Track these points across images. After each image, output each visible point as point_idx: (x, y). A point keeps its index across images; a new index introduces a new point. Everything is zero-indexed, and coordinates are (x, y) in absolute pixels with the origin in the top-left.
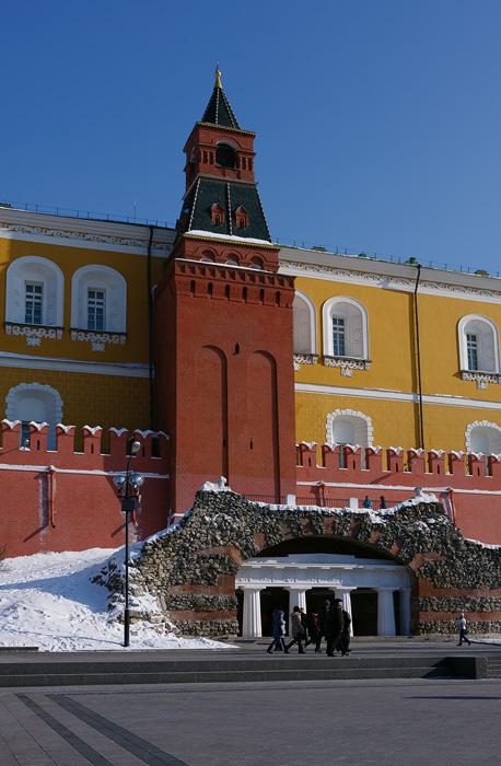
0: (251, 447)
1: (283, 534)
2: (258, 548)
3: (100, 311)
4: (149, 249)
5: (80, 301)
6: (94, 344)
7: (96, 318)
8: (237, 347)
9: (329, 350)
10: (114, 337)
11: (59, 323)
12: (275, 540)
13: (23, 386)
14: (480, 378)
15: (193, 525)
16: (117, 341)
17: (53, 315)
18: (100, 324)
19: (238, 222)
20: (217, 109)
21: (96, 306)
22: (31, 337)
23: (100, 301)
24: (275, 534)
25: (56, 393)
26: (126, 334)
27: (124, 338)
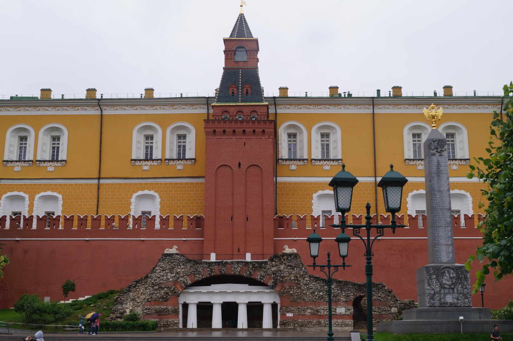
0: (247, 220)
1: (205, 273)
2: (189, 282)
4: (208, 109)
5: (171, 143)
7: (181, 149)
8: (240, 164)
9: (317, 154)
11: (160, 157)
12: (199, 277)
13: (140, 193)
14: (418, 162)
15: (158, 271)
17: (157, 154)
18: (184, 154)
19: (245, 92)
20: (241, 21)
21: (182, 144)
22: (145, 165)
23: (184, 141)
24: (199, 274)
25: (156, 194)
26: (195, 159)
27: (194, 161)
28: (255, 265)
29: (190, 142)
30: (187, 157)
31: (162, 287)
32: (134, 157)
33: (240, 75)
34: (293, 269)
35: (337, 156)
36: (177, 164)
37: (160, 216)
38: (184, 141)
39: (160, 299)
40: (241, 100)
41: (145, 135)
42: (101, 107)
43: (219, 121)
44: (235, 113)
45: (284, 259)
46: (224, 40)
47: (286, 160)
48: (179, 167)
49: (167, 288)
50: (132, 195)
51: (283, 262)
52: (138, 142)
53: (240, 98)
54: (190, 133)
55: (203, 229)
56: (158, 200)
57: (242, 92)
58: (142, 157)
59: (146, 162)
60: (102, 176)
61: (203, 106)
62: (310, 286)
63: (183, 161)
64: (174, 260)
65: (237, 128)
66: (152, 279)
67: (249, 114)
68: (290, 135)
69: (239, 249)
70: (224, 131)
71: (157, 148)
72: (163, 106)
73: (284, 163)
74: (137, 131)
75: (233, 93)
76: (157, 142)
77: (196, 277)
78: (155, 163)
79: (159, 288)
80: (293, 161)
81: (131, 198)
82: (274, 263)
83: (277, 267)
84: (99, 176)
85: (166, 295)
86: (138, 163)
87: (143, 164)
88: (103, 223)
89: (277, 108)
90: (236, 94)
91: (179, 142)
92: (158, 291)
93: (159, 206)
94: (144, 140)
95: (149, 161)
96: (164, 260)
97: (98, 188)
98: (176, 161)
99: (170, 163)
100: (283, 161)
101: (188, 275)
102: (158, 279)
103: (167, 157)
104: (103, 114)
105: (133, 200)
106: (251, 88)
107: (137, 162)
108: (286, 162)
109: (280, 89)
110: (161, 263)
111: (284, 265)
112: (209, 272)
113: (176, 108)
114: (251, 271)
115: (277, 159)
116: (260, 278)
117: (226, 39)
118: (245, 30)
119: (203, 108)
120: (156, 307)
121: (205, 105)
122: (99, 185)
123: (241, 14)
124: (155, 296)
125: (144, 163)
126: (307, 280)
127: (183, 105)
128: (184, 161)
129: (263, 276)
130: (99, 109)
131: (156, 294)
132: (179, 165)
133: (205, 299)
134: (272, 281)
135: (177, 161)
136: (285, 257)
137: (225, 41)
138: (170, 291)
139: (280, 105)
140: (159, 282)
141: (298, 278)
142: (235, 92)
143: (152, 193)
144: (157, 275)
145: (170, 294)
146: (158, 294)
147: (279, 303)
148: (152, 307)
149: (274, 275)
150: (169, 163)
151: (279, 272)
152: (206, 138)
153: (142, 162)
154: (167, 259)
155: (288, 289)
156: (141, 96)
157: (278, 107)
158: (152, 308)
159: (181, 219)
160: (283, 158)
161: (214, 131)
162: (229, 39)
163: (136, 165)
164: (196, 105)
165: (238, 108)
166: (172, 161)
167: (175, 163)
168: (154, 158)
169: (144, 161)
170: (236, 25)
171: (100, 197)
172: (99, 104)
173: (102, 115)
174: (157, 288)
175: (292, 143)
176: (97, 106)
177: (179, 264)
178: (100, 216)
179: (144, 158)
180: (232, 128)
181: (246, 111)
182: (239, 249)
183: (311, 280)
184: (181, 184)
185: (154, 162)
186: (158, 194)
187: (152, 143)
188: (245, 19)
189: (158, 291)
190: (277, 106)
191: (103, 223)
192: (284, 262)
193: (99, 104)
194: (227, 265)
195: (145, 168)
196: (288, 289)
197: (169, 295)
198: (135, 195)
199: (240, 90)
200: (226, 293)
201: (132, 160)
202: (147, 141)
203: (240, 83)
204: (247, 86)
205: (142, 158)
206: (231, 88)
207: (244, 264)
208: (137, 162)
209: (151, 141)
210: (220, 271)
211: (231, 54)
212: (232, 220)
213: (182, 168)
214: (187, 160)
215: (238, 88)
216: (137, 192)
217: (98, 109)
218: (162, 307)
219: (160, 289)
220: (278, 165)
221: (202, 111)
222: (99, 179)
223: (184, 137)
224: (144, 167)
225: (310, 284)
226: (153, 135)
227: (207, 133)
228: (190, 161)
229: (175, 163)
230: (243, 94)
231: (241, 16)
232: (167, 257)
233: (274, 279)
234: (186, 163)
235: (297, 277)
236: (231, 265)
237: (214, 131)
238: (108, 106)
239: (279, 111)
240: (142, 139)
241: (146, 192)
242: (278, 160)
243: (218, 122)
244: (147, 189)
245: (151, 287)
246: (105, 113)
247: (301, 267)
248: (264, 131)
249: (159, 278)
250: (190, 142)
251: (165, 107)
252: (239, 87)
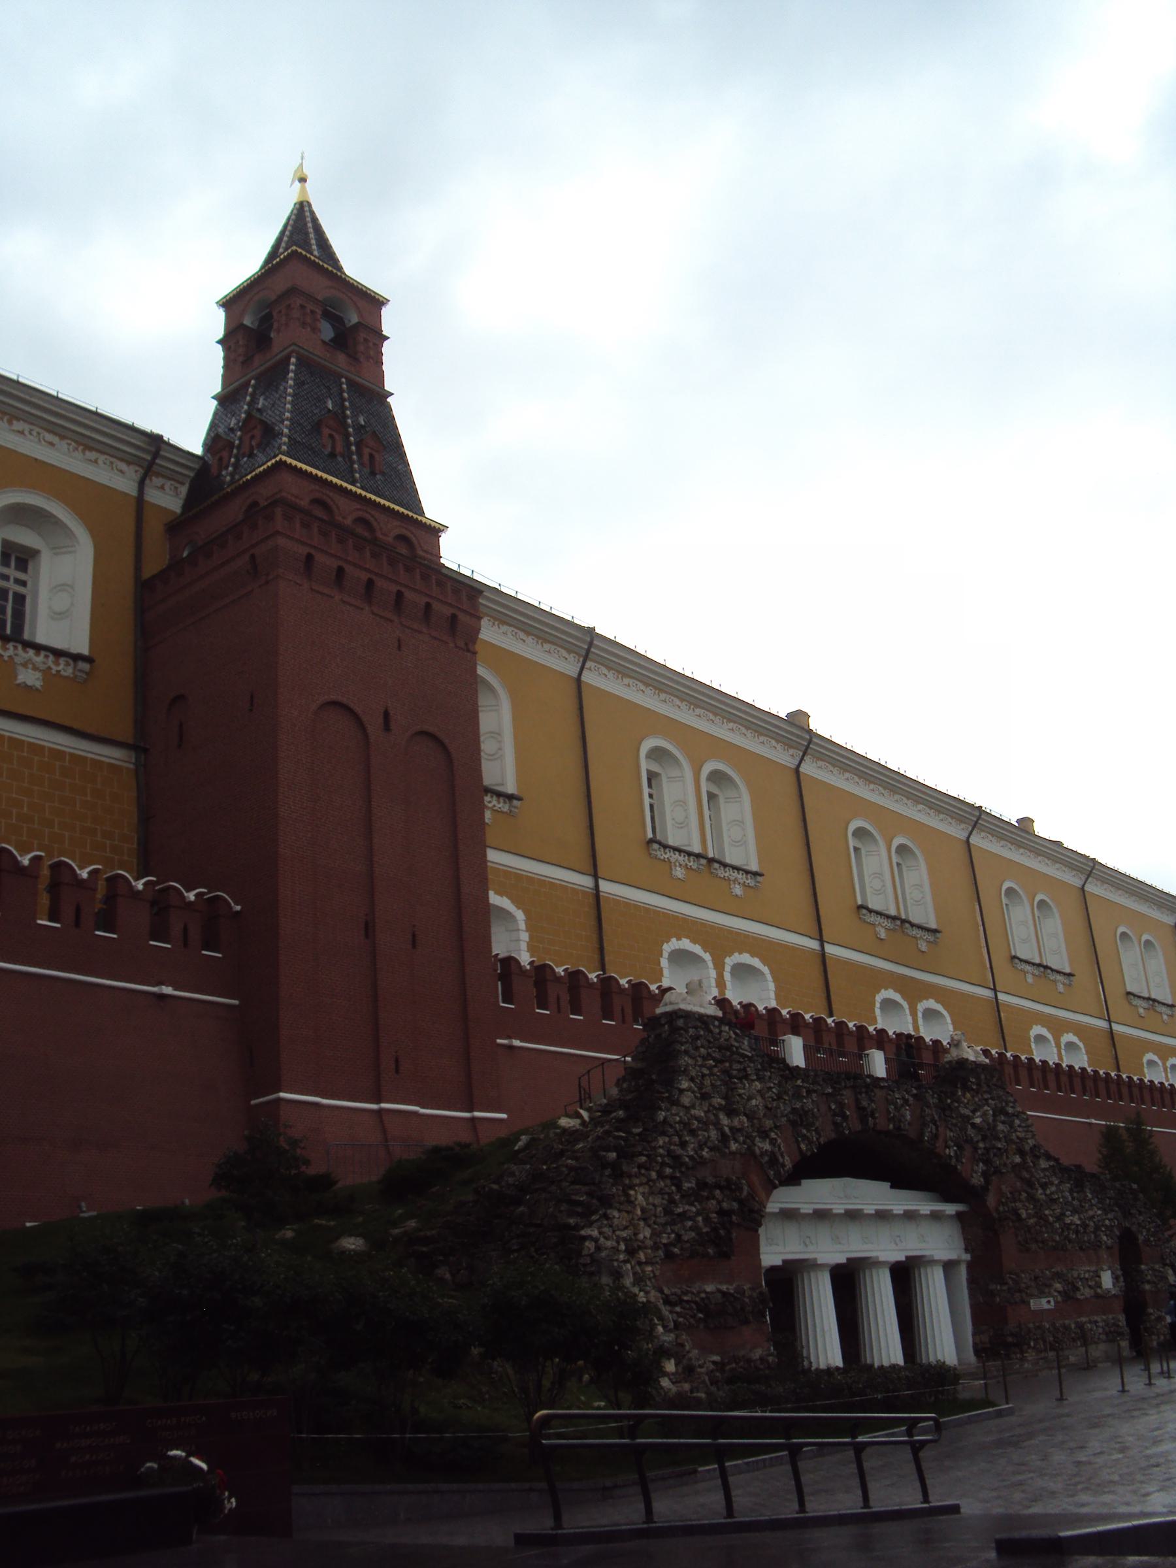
6: (20, 669)
10: (62, 661)
16: (69, 672)
19: (366, 458)
27: (85, 666)
35: (502, 785)
36: (17, 660)
113: (22, 433)
127: (49, 431)
132: (25, 665)
184: (35, 749)
212: (367, 936)
213: (38, 684)
221: (123, 481)
229: (11, 652)
234: (55, 668)
245: (668, 1182)
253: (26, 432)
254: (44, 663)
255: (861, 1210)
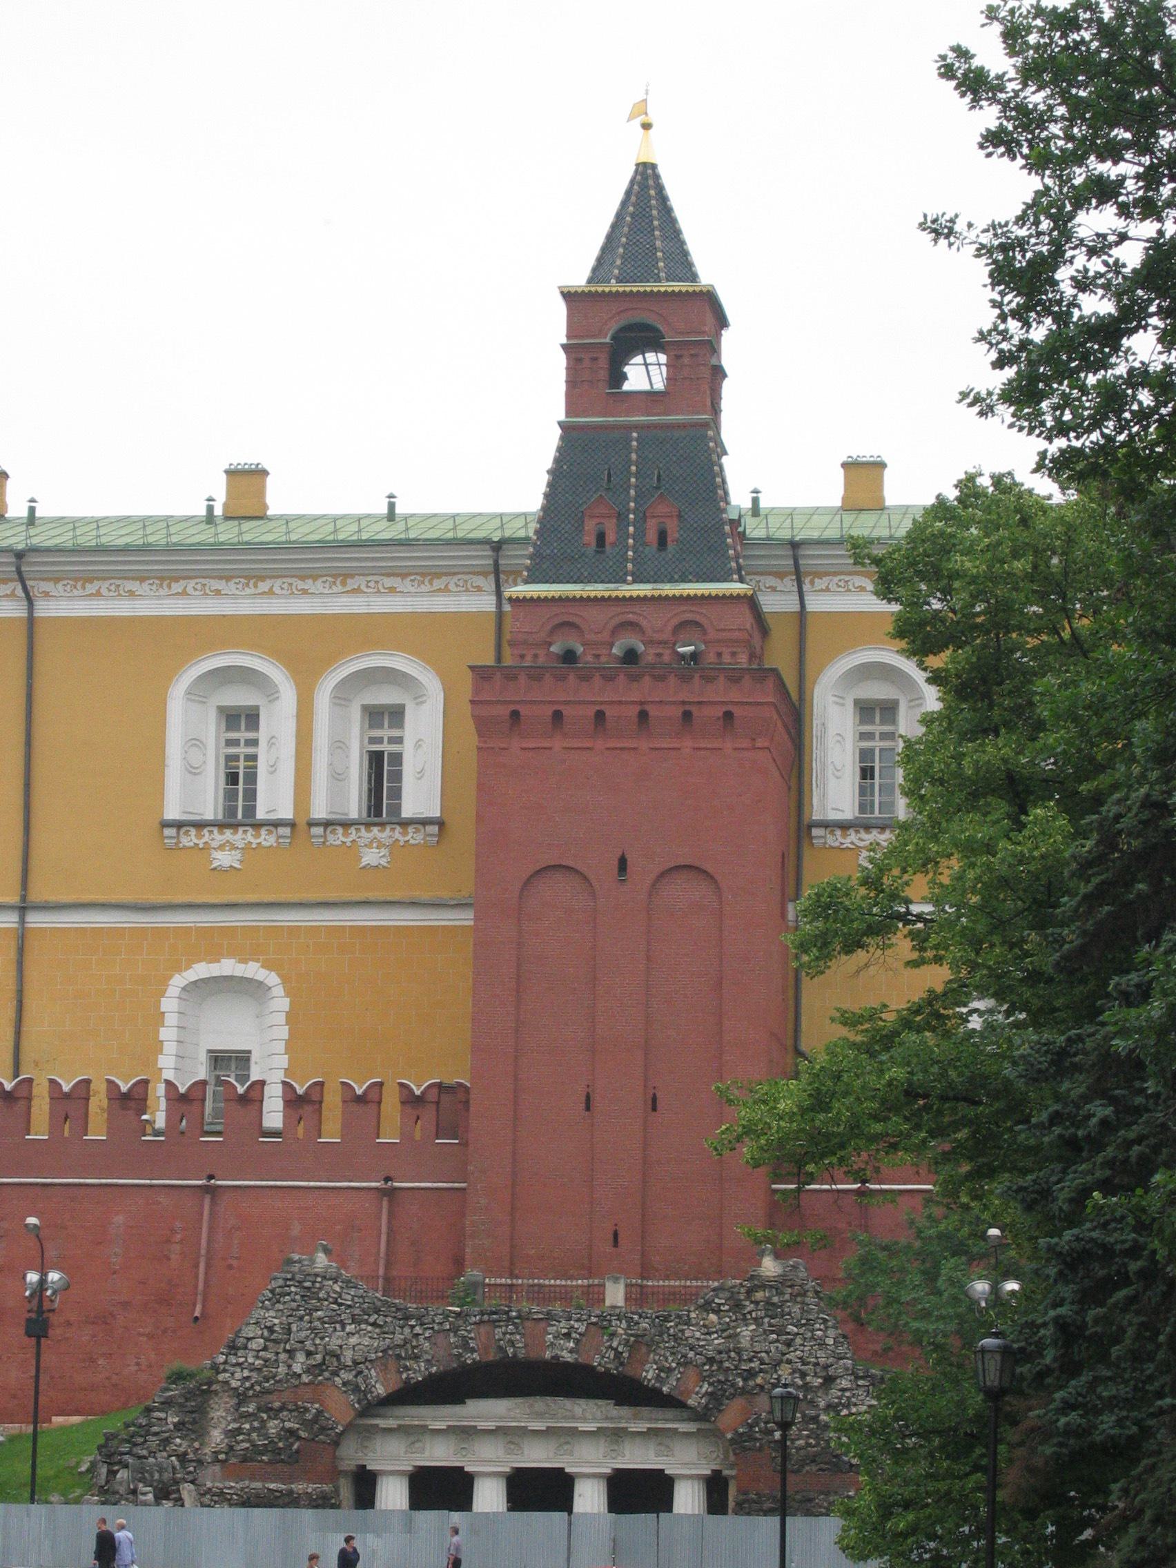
0: (654, 1109)
2: (381, 1390)
3: (397, 759)
4: (499, 593)
5: (339, 745)
8: (623, 864)
11: (286, 812)
12: (418, 1372)
13: (202, 970)
15: (253, 1345)
19: (652, 536)
22: (221, 847)
23: (395, 733)
25: (272, 979)
26: (440, 823)
27: (434, 829)
28: (637, 1323)
29: (418, 744)
30: (407, 811)
31: (271, 1409)
32: (172, 813)
33: (634, 456)
34: (789, 1344)
36: (361, 842)
37: (284, 1083)
38: (395, 733)
39: (263, 1455)
40: (633, 574)
41: (221, 710)
42: (29, 583)
43: (536, 674)
44: (605, 636)
45: (757, 1303)
46: (562, 293)
47: (844, 826)
48: (371, 857)
49: (291, 1411)
50: (164, 982)
51: (750, 1313)
52: (195, 742)
53: (630, 566)
54: (419, 699)
55: (465, 1144)
56: (280, 1003)
57: (639, 536)
58: (210, 808)
59: (228, 832)
60: (35, 896)
61: (479, 581)
62: (854, 1410)
63: (388, 828)
64: (319, 1300)
65: (612, 703)
66: (233, 1374)
67: (666, 635)
68: (865, 710)
69: (616, 1235)
70: (558, 716)
71: (273, 769)
72: (303, 578)
73: (835, 839)
74: (188, 693)
75: (601, 538)
76: (272, 741)
77: (407, 1369)
78: (267, 839)
79: (259, 1409)
80: (875, 832)
81: (162, 994)
82: (713, 1317)
83: (724, 1335)
84: (24, 898)
85: (287, 1439)
86: (190, 839)
87: (214, 844)
88: (41, 1107)
89: (806, 587)
90: (613, 544)
91: (373, 740)
92: (256, 1424)
93: (284, 1032)
94: (218, 725)
95: (241, 830)
96: (279, 1302)
97: (21, 951)
98: (358, 830)
99: (331, 839)
100: (832, 833)
101: (370, 1361)
102: (254, 1374)
103: (320, 811)
104: (38, 614)
105: (169, 1004)
106: (680, 516)
107: (187, 833)
108: (845, 836)
109: (851, 467)
110: (268, 1310)
111: (753, 1327)
112: (455, 1351)
114: (620, 1349)
115: (806, 821)
116: (658, 1375)
117: (573, 290)
118: (658, 243)
119: (479, 589)
120: (247, 1483)
121: (485, 574)
122: (22, 937)
123: (644, 164)
124: (242, 1441)
125: (218, 837)
126: (843, 1390)
127: (389, 575)
128: (393, 830)
129: (670, 1370)
130: (20, 592)
131: (249, 1435)
132: (369, 846)
133: (439, 1454)
134: (704, 1390)
135: (363, 828)
136: (759, 1295)
137: (570, 296)
138: (304, 1423)
139: (821, 575)
140: (258, 1388)
141: (808, 1379)
142: (611, 537)
143: (252, 970)
144: (250, 1360)
145: (303, 1434)
146: (254, 1435)
147: (733, 1477)
148: (233, 1484)
149: (711, 1366)
150: (325, 836)
151: (733, 1354)
152: (479, 749)
153: (211, 832)
154: (289, 1294)
155: (766, 1423)
156: (210, 509)
157: (812, 583)
158: (231, 1488)
159: (368, 1101)
160: (833, 816)
161: (515, 715)
162: (586, 290)
163: (185, 848)
164: (446, 574)
165: (619, 610)
166: (340, 830)
167: (353, 837)
168: (261, 814)
169: (215, 830)
170: (619, 216)
171: (26, 987)
172: (19, 572)
173: (31, 621)
174: (251, 1410)
175: (877, 744)
176: (12, 580)
177: (340, 1315)
178: (30, 1081)
179: (220, 817)
180: (593, 703)
181: (654, 621)
182: (616, 1235)
183: (858, 1385)
185: (263, 831)
186: (279, 975)
187: (254, 743)
188: (660, 189)
189: (256, 1424)
190: (807, 580)
191: (41, 1107)
192: (754, 1315)
193: (19, 572)
194: (528, 1324)
195: (224, 859)
196: (766, 1423)
197: (299, 1438)
198: (178, 981)
199: (631, 529)
200: (524, 1432)
201: (166, 824)
202: (233, 735)
203: (632, 492)
204: (661, 509)
205: (209, 816)
206: (591, 517)
207: (594, 1319)
208: (187, 833)
209: (251, 735)
210: (500, 1348)
211: (596, 359)
213: (383, 862)
214: (405, 824)
215: (621, 517)
216: (188, 967)
217: (13, 595)
218: (272, 1486)
219: (265, 1416)
220: (807, 854)
222: (23, 909)
223: (396, 715)
224: (218, 855)
225: (855, 1405)
226: (257, 708)
227: (483, 726)
228: (417, 831)
229: (353, 837)
230: (645, 544)
231: (645, 177)
232: (289, 1286)
233: (710, 1384)
234: (402, 839)
235: (803, 1375)
236: (543, 1324)
237: (515, 715)
238: (57, 580)
239: (816, 604)
240: (210, 730)
241: (228, 967)
242: (810, 827)
243: (530, 677)
244: (231, 954)
246: (45, 609)
247: (820, 1333)
248: (728, 715)
249: (259, 1370)
250: (418, 744)
251: (308, 584)
252: (628, 511)
253: (363, 588)
254: (390, 837)
255: (475, 1427)
